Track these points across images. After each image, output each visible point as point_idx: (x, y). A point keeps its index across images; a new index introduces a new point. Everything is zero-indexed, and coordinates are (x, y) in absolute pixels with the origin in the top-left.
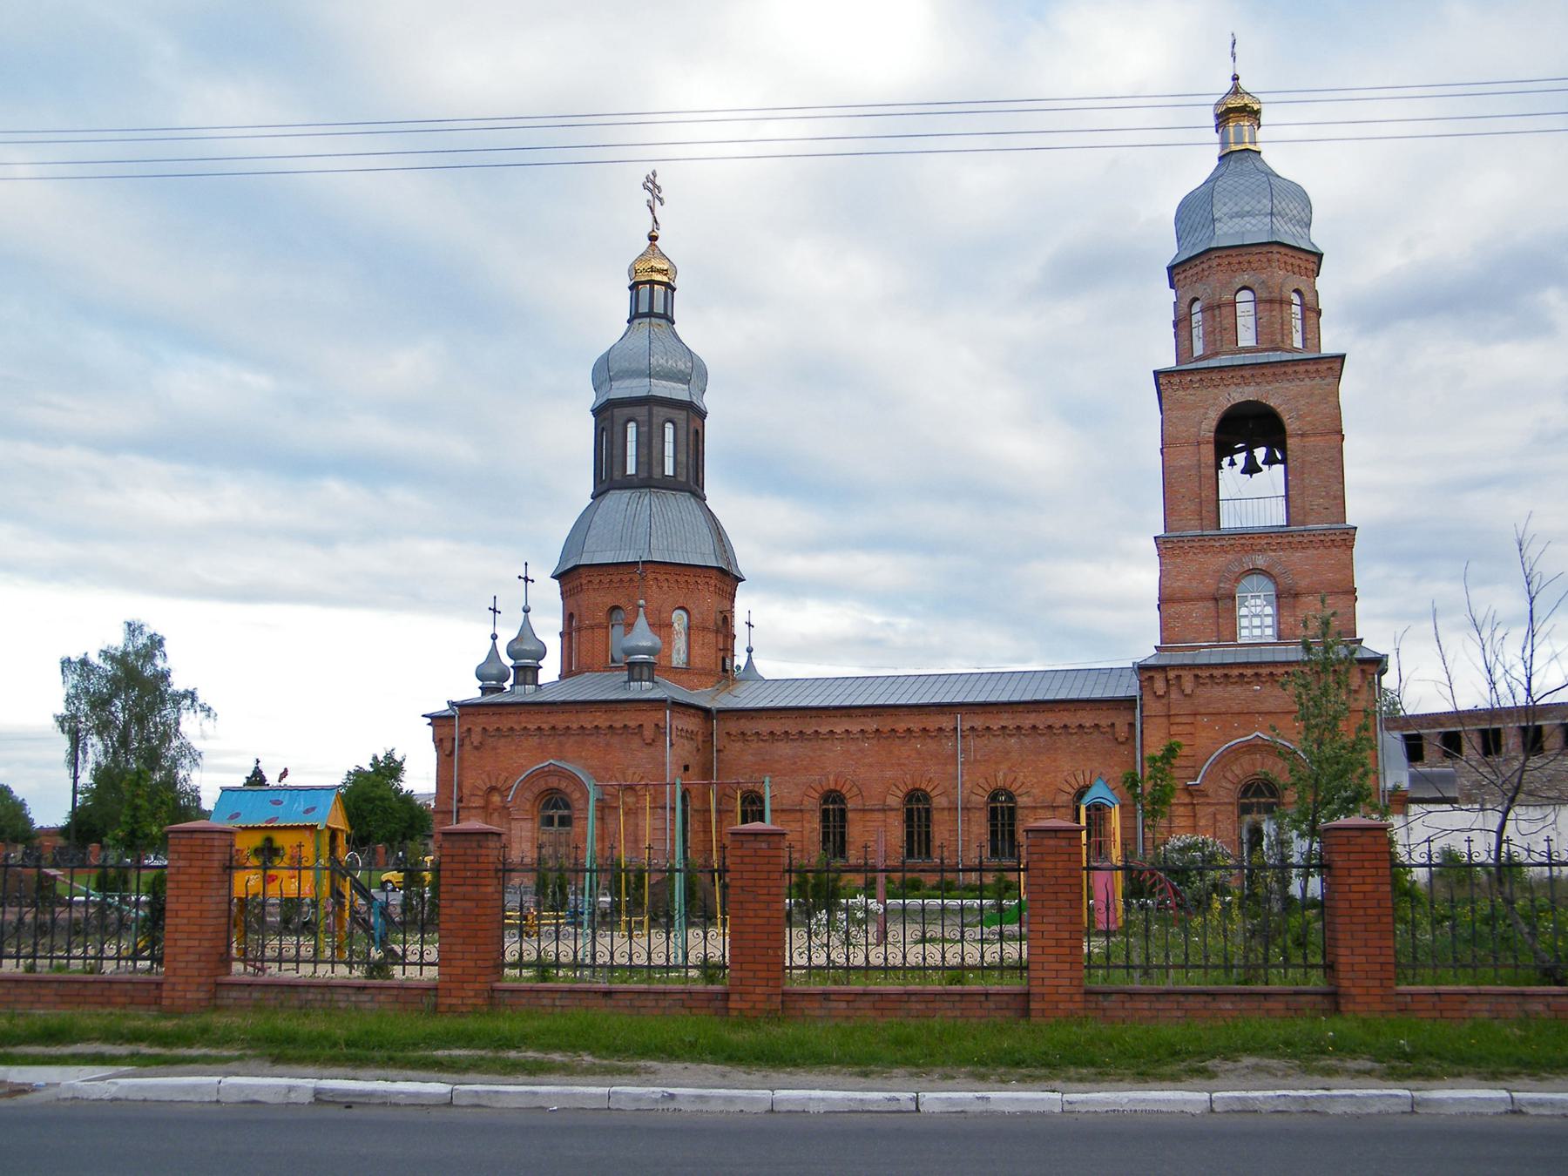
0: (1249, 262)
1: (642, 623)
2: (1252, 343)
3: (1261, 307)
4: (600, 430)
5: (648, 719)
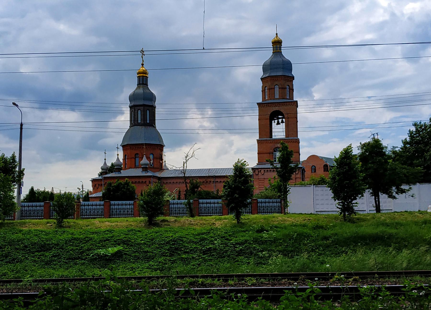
0: (278, 79)
1: (145, 157)
2: (278, 97)
3: (280, 89)
4: (131, 112)
5: (147, 180)
